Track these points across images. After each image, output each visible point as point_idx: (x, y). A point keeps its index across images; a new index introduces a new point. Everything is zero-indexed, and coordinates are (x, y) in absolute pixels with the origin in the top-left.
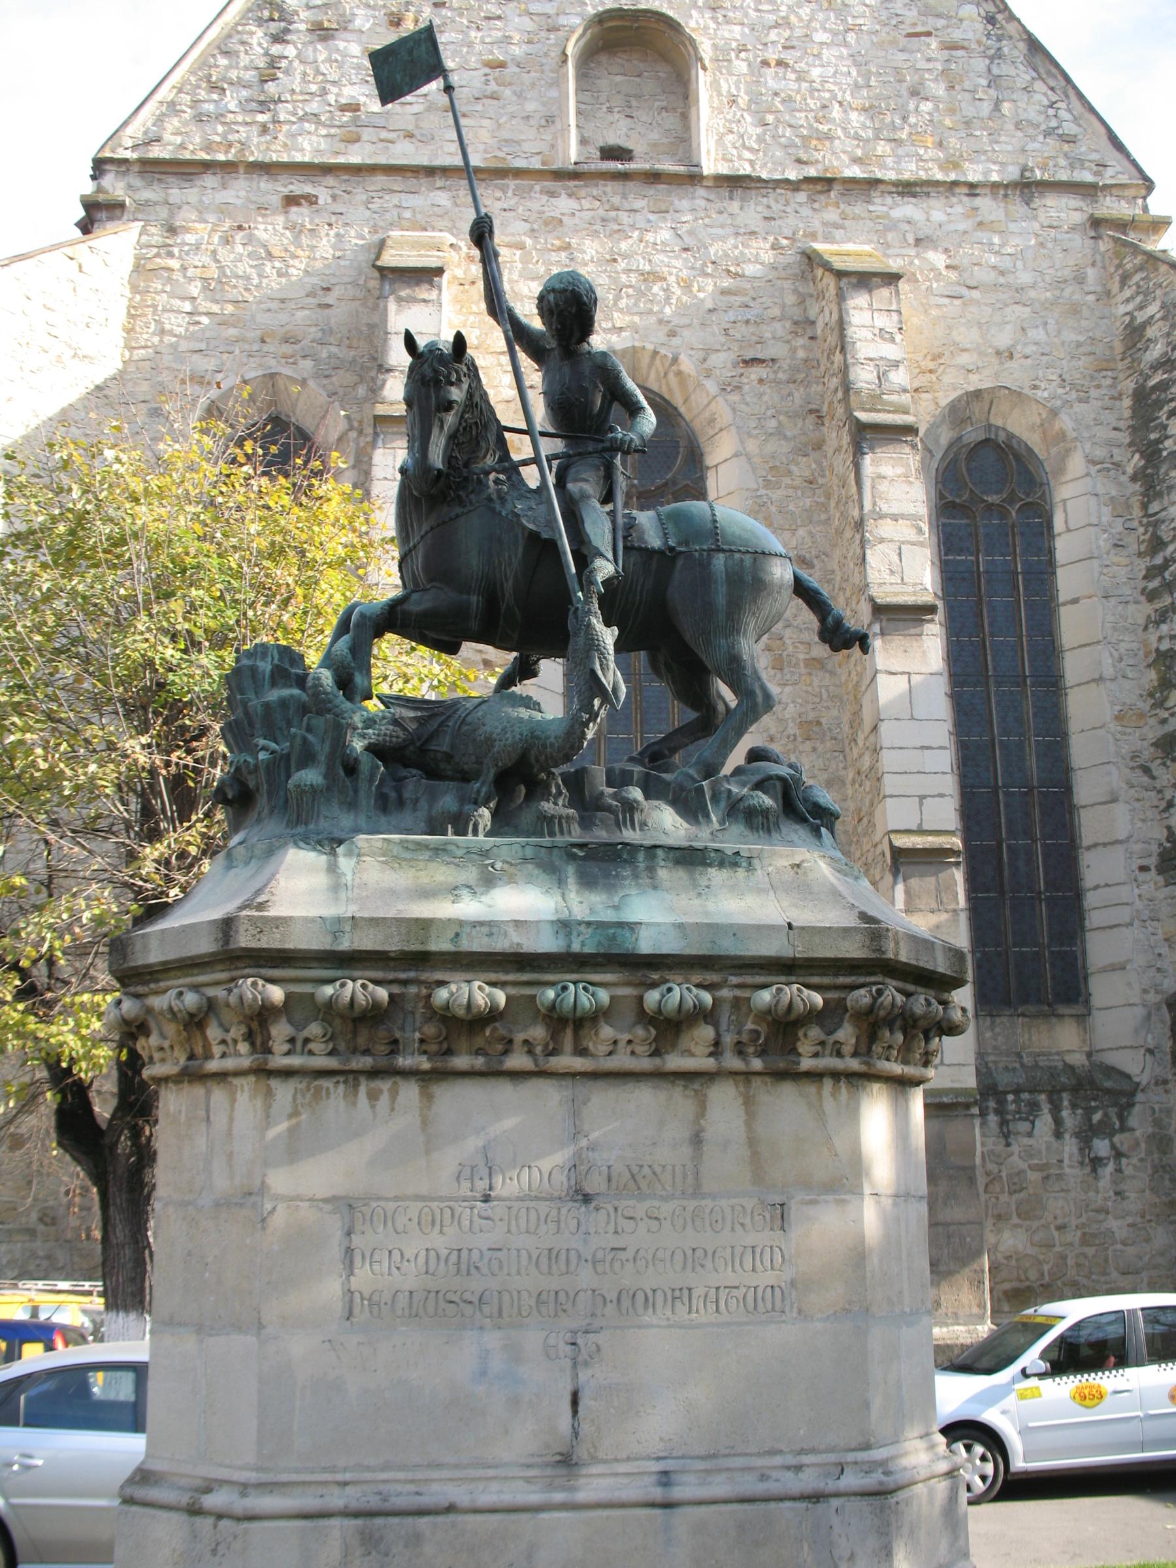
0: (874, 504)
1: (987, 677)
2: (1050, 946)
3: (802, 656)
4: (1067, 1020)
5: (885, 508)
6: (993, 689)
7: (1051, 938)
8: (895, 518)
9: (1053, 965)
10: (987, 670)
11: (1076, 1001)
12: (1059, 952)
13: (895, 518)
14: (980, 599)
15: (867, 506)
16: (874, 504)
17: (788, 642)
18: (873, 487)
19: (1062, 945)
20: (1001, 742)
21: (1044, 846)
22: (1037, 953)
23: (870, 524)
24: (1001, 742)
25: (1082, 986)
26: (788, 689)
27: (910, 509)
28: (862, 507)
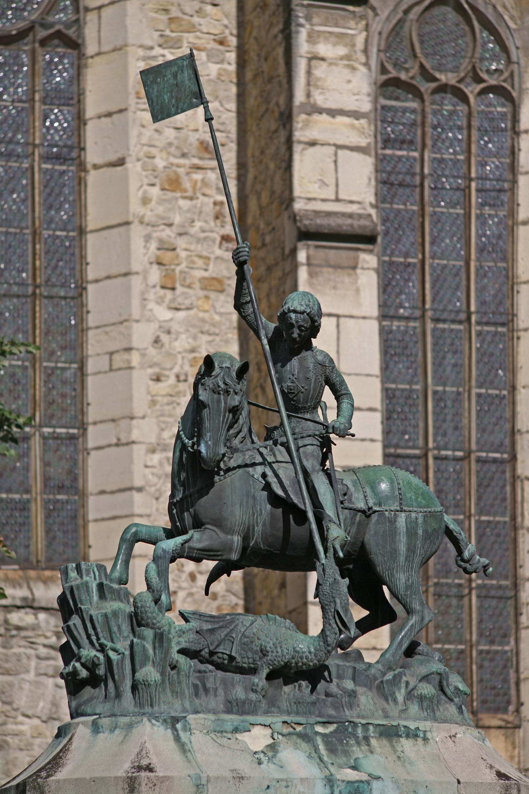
0: (308, 95)
1: (424, 311)
2: (478, 643)
3: (199, 274)
4: (493, 732)
5: (319, 99)
6: (430, 325)
7: (481, 634)
8: (333, 113)
9: (480, 667)
10: (424, 302)
11: (505, 711)
12: (488, 652)
13: (333, 113)
14: (423, 209)
15: (299, 97)
16: (308, 95)
17: (183, 254)
18: (309, 73)
19: (492, 642)
20: (435, 393)
21: (479, 523)
22: (462, 652)
23: (300, 119)
24: (435, 393)
25: (513, 692)
26: (181, 315)
27: (351, 104)
28: (290, 96)
